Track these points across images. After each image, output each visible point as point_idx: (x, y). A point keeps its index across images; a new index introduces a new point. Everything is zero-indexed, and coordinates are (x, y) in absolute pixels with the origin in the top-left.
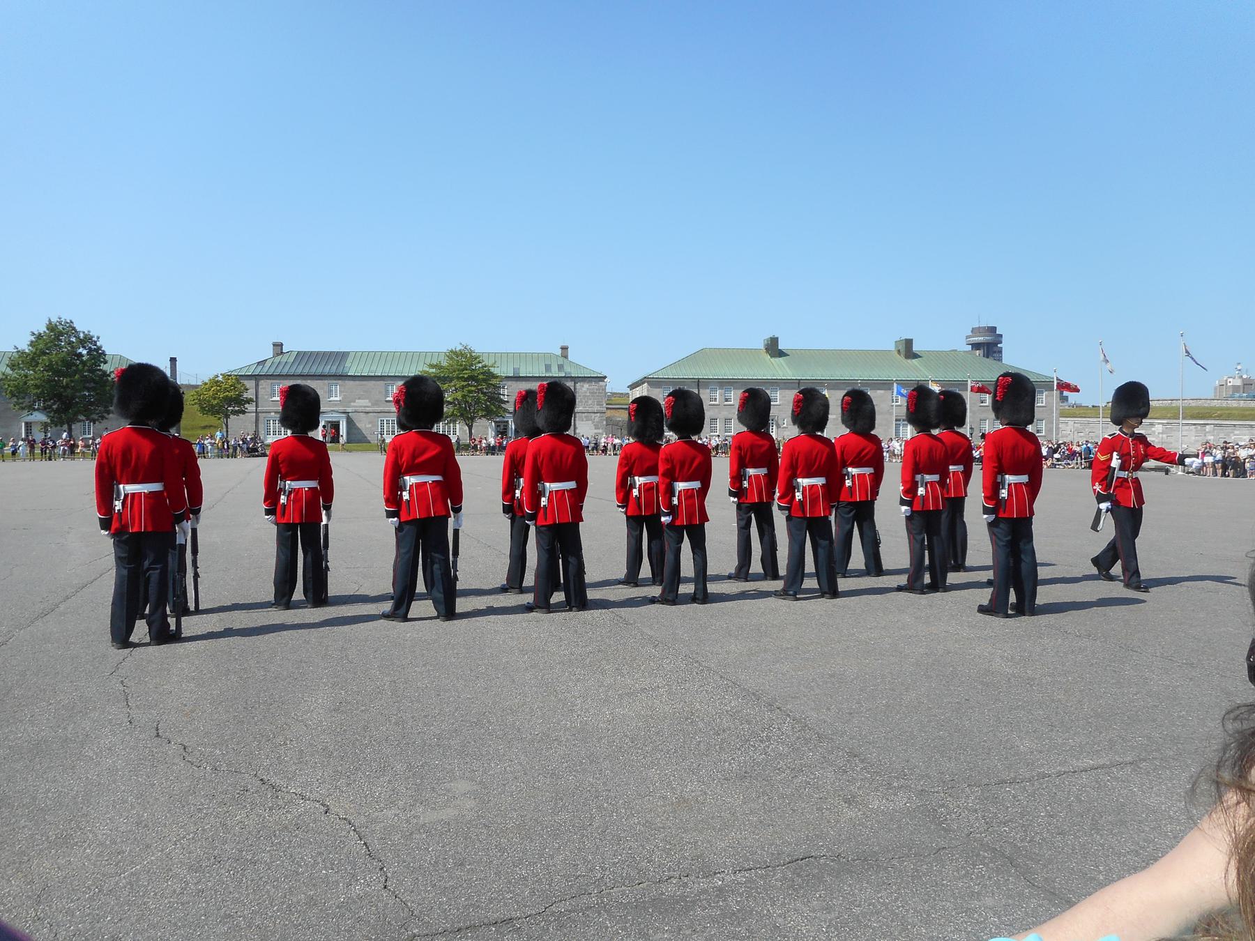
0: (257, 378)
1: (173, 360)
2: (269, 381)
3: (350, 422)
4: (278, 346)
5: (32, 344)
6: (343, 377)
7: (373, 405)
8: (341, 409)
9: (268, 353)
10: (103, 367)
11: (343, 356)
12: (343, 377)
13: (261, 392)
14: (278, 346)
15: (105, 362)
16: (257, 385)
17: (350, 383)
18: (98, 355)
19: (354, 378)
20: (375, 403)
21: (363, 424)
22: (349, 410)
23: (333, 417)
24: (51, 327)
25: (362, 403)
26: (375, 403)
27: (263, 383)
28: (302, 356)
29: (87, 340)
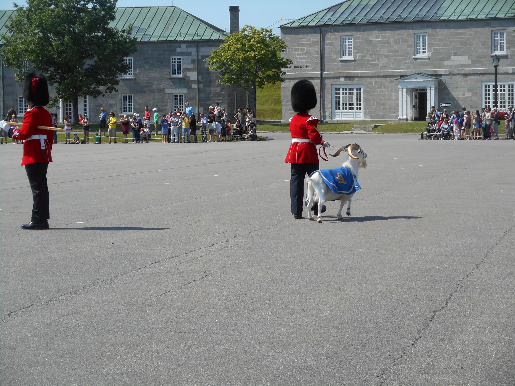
0: (321, 29)
1: (234, 11)
2: (338, 34)
3: (442, 91)
8: (430, 70)
10: (111, 25)
13: (328, 49)
15: (113, 18)
16: (322, 41)
17: (443, 33)
19: (448, 23)
20: (477, 61)
21: (462, 92)
22: (441, 71)
23: (419, 82)
25: (460, 61)
26: (477, 61)
27: (332, 39)
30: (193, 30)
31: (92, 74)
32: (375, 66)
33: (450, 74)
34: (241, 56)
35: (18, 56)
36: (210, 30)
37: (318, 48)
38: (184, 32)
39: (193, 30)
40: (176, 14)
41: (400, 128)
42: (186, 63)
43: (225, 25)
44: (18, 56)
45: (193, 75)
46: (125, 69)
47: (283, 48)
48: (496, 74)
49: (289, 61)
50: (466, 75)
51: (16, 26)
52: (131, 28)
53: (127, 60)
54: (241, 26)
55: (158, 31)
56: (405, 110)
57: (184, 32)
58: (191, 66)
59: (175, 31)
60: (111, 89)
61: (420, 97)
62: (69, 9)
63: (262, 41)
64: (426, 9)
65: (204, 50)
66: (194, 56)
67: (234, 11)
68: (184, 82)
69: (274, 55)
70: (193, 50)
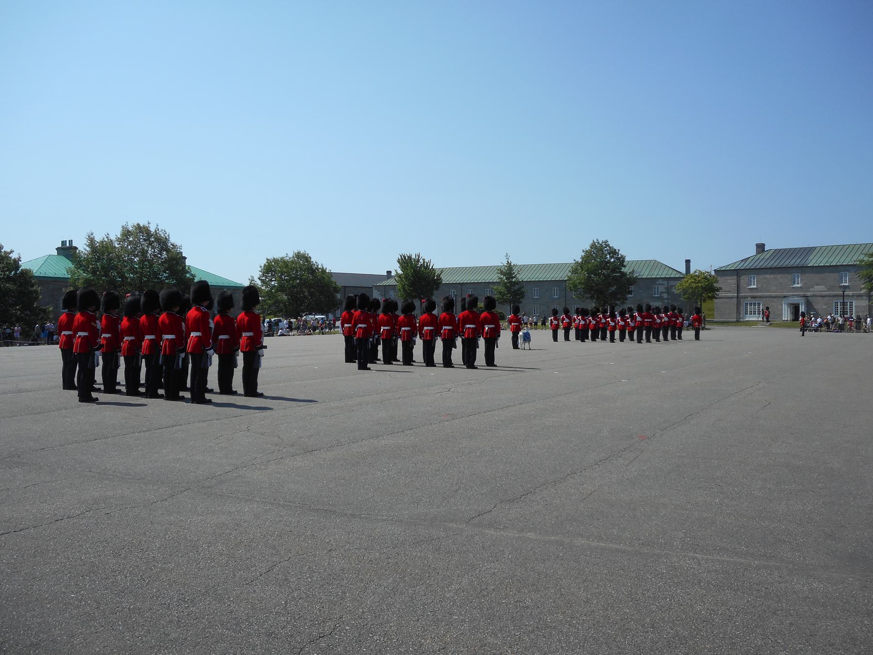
0: (737, 273)
1: (688, 262)
3: (809, 305)
4: (761, 248)
5: (582, 258)
6: (803, 269)
7: (829, 290)
9: (753, 252)
10: (623, 269)
11: (808, 251)
12: (803, 269)
13: (742, 282)
14: (761, 248)
15: (625, 266)
18: (621, 261)
22: (808, 294)
23: (795, 300)
24: (593, 246)
25: (819, 289)
28: (778, 253)
29: (614, 252)
30: (665, 272)
31: (613, 295)
32: (768, 291)
33: (814, 296)
34: (694, 285)
35: (575, 286)
36: (675, 272)
37: (735, 281)
38: (660, 273)
39: (665, 272)
40: (656, 264)
41: (784, 325)
42: (661, 289)
43: (683, 270)
44: (575, 286)
45: (665, 296)
46: (630, 292)
47: (717, 282)
48: (844, 296)
49: (721, 288)
50: (823, 296)
51: (574, 271)
52: (633, 271)
53: (632, 288)
54: (692, 271)
55: (647, 273)
56: (787, 315)
57: (660, 273)
58: (664, 291)
59: (656, 273)
60: (623, 303)
61: (795, 308)
62: (601, 262)
63: (706, 278)
64: (799, 261)
65: (672, 283)
66: (666, 286)
67: (688, 262)
68: (660, 298)
69: (712, 285)
70: (665, 282)
